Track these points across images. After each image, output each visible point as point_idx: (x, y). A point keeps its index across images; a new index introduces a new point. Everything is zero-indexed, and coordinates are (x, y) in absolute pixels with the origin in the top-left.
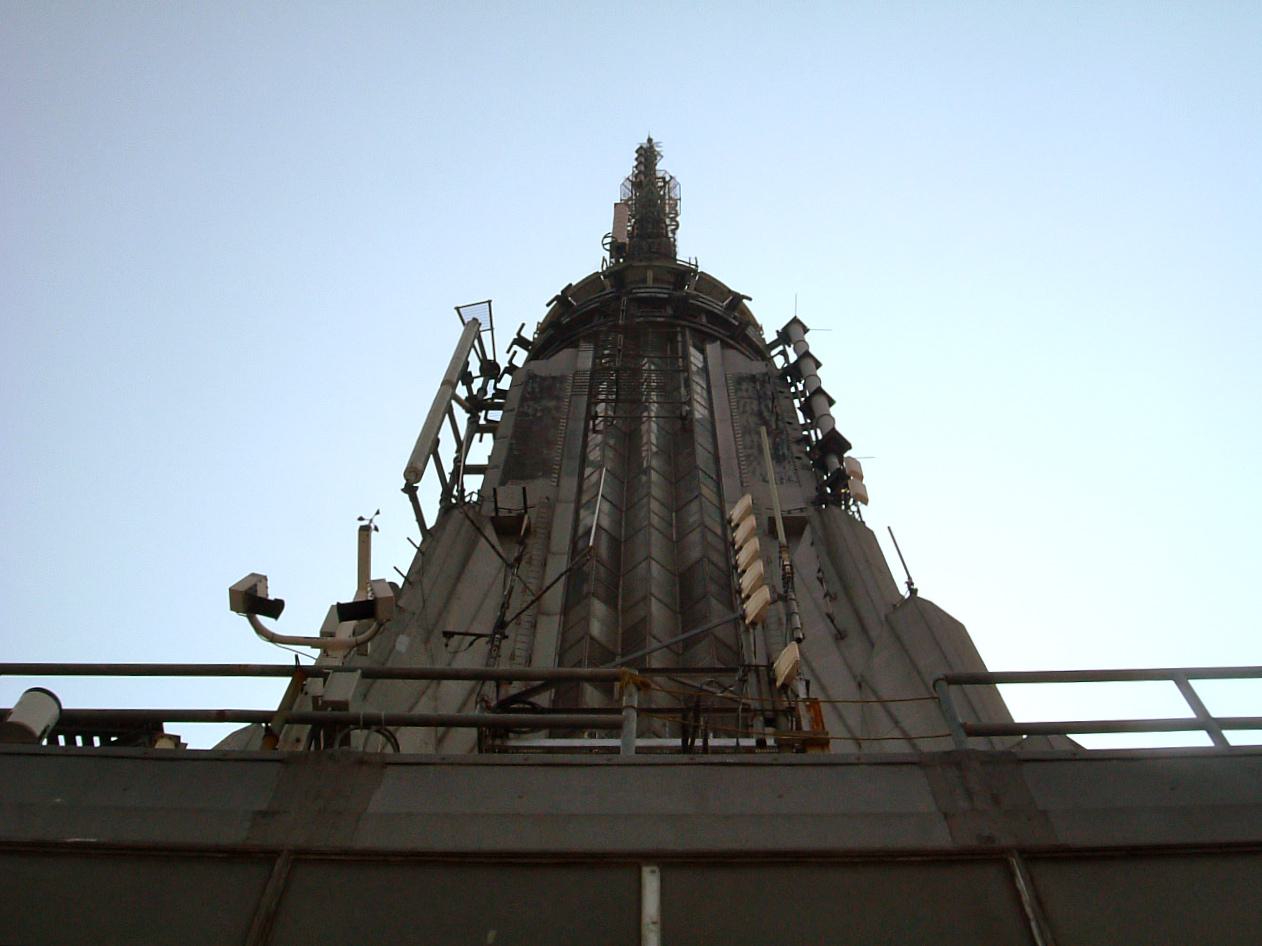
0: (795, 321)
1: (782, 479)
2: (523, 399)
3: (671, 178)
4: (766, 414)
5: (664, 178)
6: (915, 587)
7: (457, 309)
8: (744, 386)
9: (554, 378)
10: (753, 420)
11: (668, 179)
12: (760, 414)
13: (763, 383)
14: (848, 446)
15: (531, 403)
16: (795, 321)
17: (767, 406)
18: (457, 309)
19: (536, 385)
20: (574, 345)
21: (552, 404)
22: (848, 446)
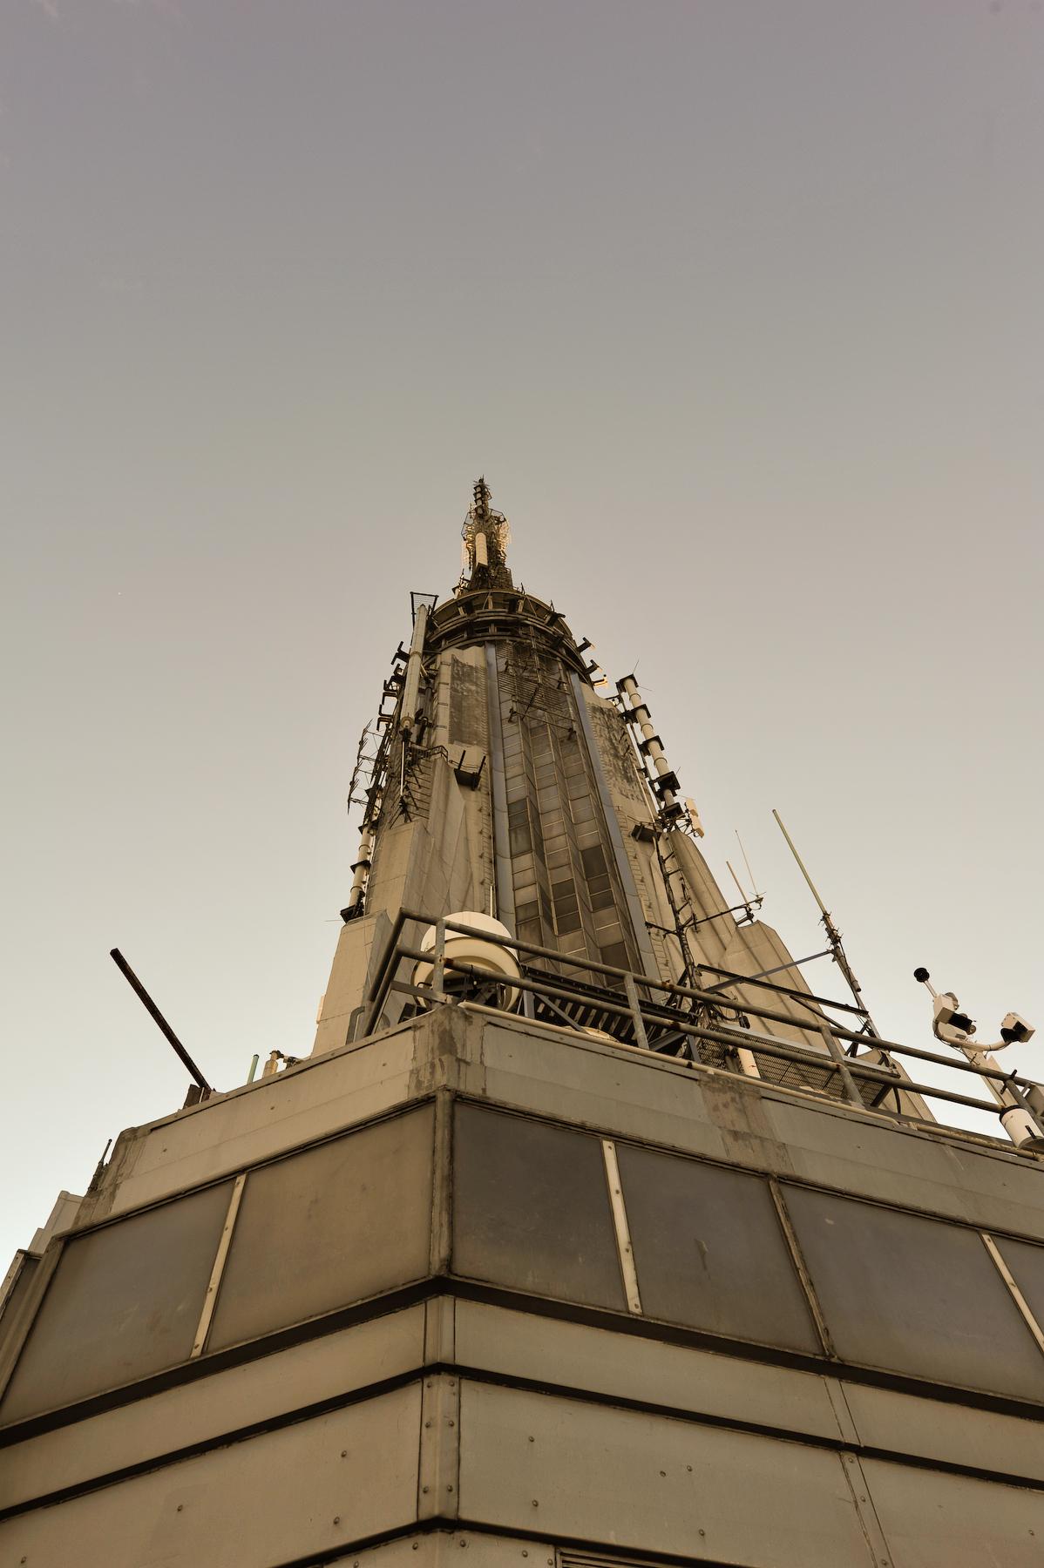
0: (632, 677)
1: (632, 795)
2: (453, 678)
3: (505, 520)
4: (614, 741)
5: (499, 518)
6: (751, 912)
7: (412, 593)
8: (598, 715)
9: (470, 666)
10: (607, 743)
11: (502, 520)
12: (610, 740)
13: (609, 716)
14: (679, 788)
15: (459, 682)
16: (632, 677)
17: (614, 735)
18: (412, 593)
19: (459, 669)
20: (480, 644)
21: (473, 688)
22: (679, 788)
